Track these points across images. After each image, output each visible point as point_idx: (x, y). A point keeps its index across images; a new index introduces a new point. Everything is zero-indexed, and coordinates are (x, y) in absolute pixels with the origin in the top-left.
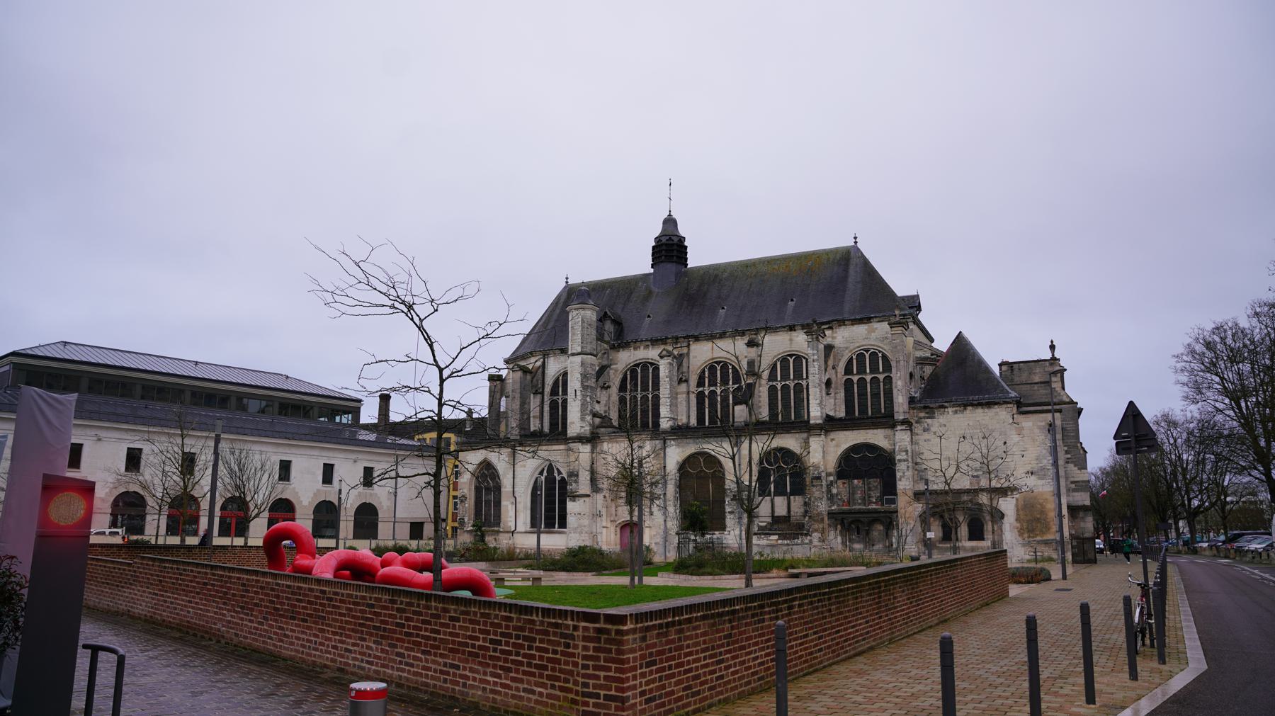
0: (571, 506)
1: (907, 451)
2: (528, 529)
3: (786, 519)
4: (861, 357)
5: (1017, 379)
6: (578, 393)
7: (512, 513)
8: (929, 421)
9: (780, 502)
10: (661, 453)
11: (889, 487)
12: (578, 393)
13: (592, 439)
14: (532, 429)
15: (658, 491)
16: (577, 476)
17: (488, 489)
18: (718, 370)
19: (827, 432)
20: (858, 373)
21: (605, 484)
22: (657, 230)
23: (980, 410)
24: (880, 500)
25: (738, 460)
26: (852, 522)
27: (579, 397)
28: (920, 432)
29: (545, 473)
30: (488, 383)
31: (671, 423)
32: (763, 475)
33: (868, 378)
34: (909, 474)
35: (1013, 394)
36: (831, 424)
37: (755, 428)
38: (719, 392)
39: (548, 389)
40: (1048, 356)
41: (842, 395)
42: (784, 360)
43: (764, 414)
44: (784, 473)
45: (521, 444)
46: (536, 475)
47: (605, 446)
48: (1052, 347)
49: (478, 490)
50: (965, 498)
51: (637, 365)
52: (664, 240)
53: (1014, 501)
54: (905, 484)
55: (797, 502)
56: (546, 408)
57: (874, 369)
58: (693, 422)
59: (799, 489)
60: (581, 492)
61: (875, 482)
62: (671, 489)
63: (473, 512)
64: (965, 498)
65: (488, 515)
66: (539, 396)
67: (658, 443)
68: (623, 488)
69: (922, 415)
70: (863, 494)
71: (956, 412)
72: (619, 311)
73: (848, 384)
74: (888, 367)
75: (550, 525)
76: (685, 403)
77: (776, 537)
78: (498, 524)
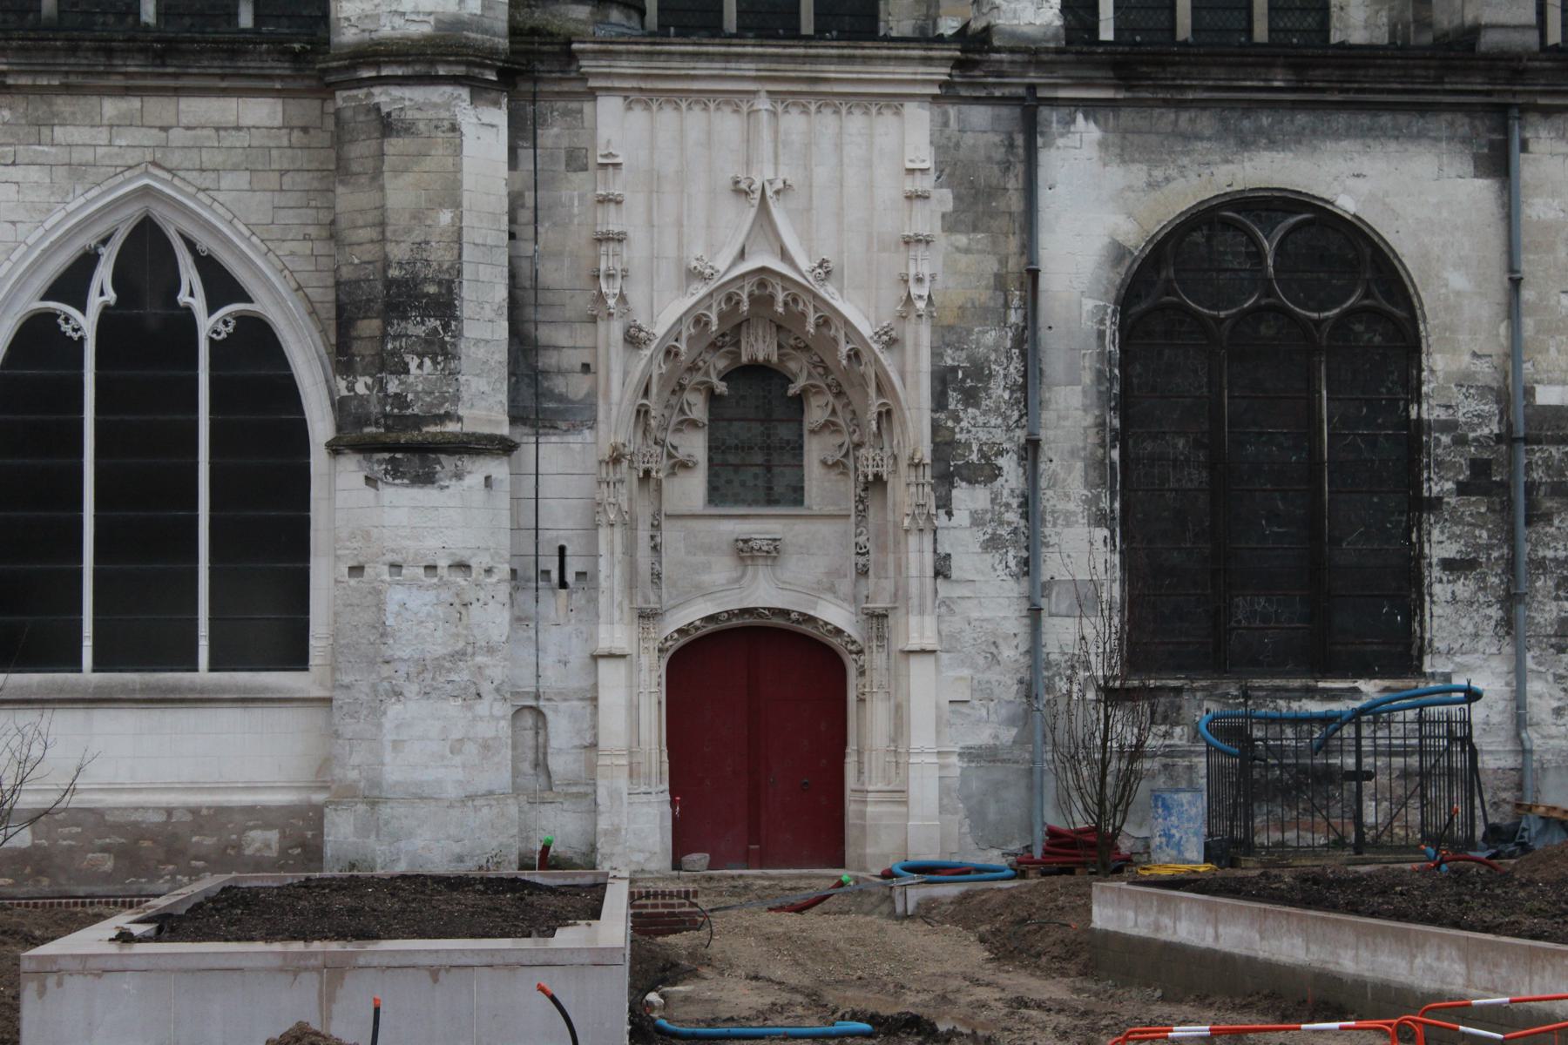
15: (980, 428)
16: (445, 306)
29: (102, 291)
47: (615, 125)
62: (1072, 412)
67: (981, 125)
68: (699, 409)
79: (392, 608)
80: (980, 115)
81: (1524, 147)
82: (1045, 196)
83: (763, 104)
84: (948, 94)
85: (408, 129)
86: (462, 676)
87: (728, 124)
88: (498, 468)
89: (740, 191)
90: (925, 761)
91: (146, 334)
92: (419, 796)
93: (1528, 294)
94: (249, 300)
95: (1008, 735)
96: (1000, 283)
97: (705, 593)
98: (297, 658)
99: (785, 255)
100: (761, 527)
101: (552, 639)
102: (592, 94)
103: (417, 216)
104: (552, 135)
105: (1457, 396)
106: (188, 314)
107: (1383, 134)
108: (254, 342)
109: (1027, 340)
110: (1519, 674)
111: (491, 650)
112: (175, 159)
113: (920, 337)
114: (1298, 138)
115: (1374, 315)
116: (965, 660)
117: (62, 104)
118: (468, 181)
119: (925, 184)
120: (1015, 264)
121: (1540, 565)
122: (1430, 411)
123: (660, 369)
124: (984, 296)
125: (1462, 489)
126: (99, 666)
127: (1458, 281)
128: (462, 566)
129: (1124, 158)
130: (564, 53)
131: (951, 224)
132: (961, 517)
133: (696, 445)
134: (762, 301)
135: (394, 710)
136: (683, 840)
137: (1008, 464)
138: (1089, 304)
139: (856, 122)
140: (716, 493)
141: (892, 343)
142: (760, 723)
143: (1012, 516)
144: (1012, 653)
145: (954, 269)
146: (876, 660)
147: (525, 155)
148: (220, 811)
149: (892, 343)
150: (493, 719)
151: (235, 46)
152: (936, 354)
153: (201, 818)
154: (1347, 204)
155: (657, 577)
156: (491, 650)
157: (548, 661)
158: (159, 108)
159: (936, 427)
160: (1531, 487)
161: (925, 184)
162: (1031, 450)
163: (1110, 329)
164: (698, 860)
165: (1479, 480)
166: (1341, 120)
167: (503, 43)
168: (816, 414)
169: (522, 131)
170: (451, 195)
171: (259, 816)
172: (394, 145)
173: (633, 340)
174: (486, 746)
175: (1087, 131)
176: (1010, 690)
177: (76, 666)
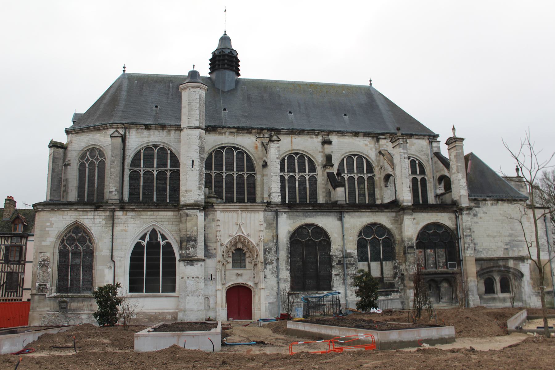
8: (477, 209)
10: (273, 225)
13: (206, 207)
15: (271, 257)
16: (195, 241)
17: (76, 254)
24: (446, 264)
25: (343, 232)
29: (147, 239)
30: (47, 152)
32: (361, 245)
37: (354, 207)
39: (128, 161)
40: (516, 175)
42: (350, 158)
47: (219, 215)
49: (63, 254)
50: (501, 263)
51: (223, 148)
53: (528, 266)
55: (388, 266)
59: (390, 256)
62: (283, 254)
64: (501, 263)
67: (270, 215)
68: (231, 255)
70: (436, 260)
71: (492, 204)
74: (423, 172)
75: (152, 288)
79: (187, 283)
80: (270, 213)
82: (279, 224)
83: (240, 212)
84: (265, 210)
85: (190, 216)
86: (197, 293)
87: (235, 215)
88: (202, 263)
89: (237, 224)
90: (263, 305)
91: (153, 245)
92: (191, 310)
93: (345, 237)
94: (167, 239)
95: (275, 300)
96: (273, 237)
97: (232, 281)
98: (174, 290)
99: (243, 233)
100: (240, 271)
101: (210, 288)
102: (216, 211)
103: (191, 228)
104: (210, 216)
105: (336, 251)
106: (159, 242)
107: (325, 215)
108: (169, 245)
109: (277, 244)
110: (346, 290)
112: (158, 220)
114: (314, 216)
115: (324, 240)
116: (269, 289)
117: (143, 213)
119: (262, 223)
120: (275, 234)
121: (348, 274)
122: (332, 253)
123: (225, 249)
125: (337, 264)
126: (146, 292)
127: (336, 235)
128: (198, 277)
129: (290, 219)
130: (212, 205)
131: (266, 228)
132: (268, 269)
133: (230, 260)
134: (240, 239)
135: (188, 298)
136: (229, 316)
137: (274, 262)
138: (285, 239)
139: (253, 214)
140: (233, 267)
142: (240, 299)
143: (275, 269)
144: (275, 289)
145: (267, 235)
146: (256, 290)
147: (207, 219)
148: (163, 313)
149: (258, 245)
151: (167, 205)
152: (264, 247)
153: (160, 314)
154: (320, 225)
155: (225, 279)
157: (209, 291)
158: (156, 213)
159: (264, 257)
160: (346, 264)
161: (262, 223)
162: (277, 260)
163: (288, 243)
164: (231, 319)
165: (339, 263)
166: (319, 213)
167: (204, 204)
168: (247, 255)
169: (206, 216)
170: (196, 225)
171: (168, 313)
172: (188, 218)
173: (222, 245)
174: (201, 303)
175: (285, 215)
176: (275, 294)
177: (142, 292)
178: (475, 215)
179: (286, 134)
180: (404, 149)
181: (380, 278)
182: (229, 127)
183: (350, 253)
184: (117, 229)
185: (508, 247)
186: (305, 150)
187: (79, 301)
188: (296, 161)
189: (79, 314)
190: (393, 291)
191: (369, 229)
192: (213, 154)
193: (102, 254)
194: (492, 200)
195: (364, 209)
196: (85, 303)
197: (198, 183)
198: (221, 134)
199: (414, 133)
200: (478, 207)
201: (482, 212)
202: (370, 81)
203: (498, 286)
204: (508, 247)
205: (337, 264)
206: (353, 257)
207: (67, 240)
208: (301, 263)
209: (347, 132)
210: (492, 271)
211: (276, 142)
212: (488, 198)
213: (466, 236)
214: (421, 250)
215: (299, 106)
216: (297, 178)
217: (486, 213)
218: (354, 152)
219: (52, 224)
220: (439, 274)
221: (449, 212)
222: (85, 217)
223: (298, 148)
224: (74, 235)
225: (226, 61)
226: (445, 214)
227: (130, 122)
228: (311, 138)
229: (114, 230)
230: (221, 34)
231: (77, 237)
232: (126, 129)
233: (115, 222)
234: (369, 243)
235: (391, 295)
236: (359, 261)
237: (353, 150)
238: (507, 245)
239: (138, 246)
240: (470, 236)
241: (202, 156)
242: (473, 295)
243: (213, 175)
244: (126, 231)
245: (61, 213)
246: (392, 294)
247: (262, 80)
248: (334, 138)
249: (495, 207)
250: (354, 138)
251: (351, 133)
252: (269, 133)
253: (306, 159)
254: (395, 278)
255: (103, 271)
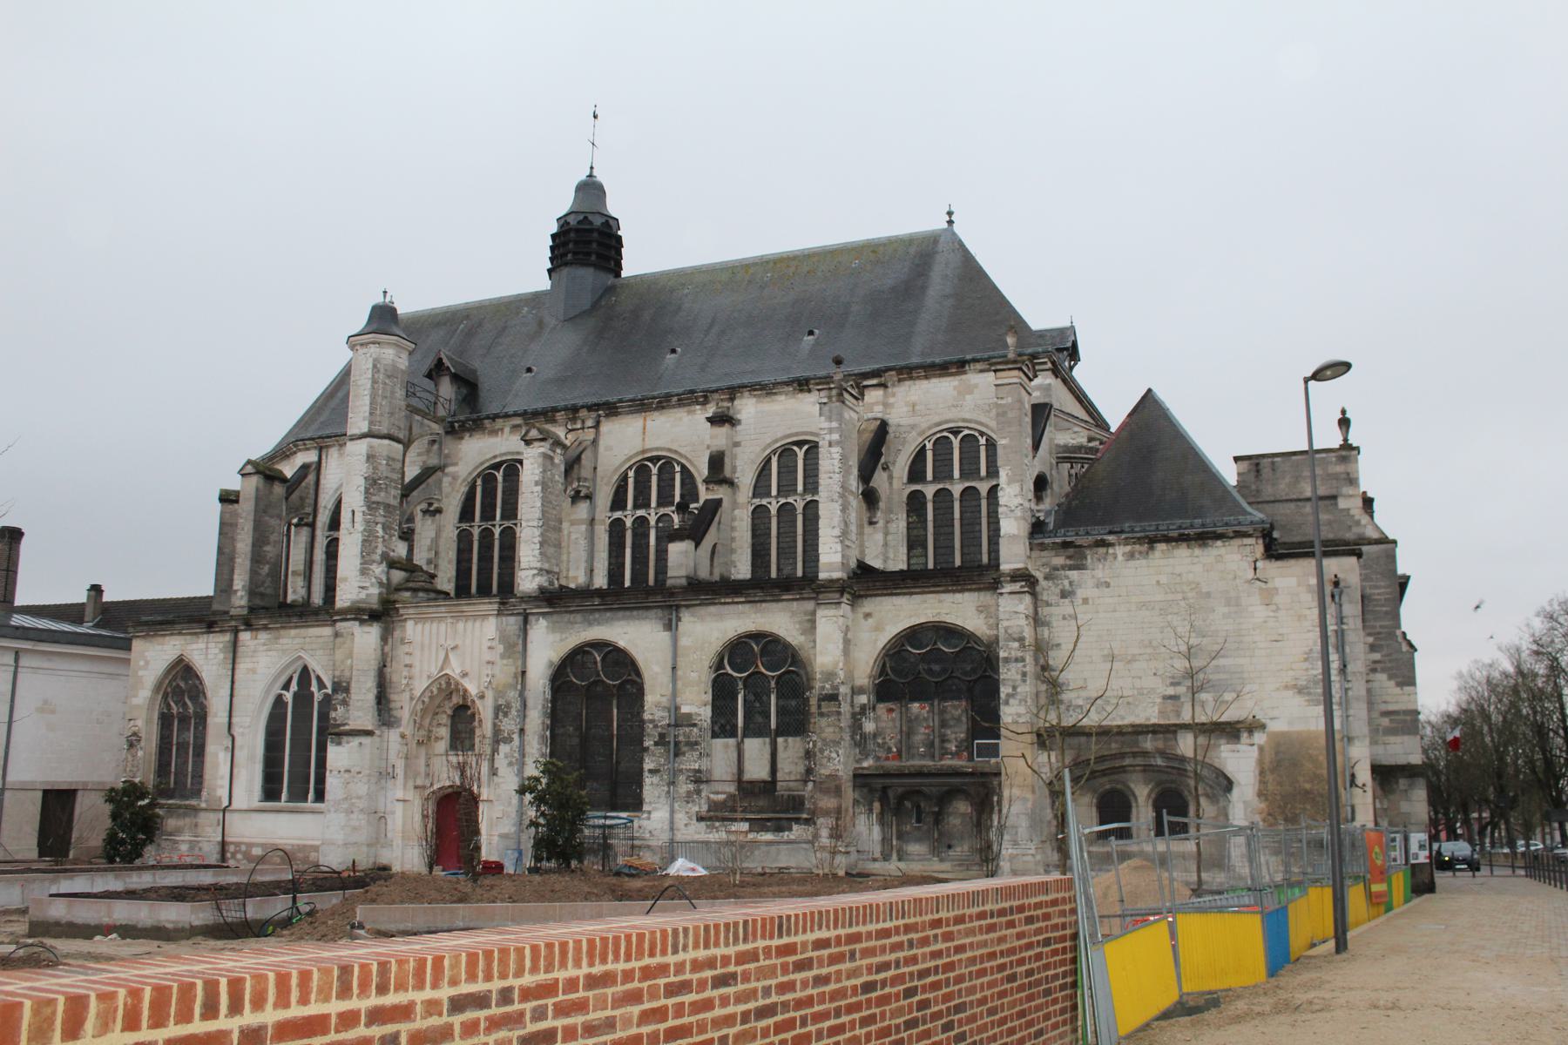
0: (338, 756)
1: (1021, 640)
2: (256, 804)
3: (769, 786)
4: (942, 445)
5: (1268, 491)
6: (359, 517)
7: (225, 770)
8: (1074, 574)
9: (755, 748)
10: (517, 647)
11: (986, 722)
12: (359, 517)
13: (383, 613)
14: (290, 598)
15: (509, 725)
16: (347, 690)
18: (653, 474)
19: (856, 598)
20: (936, 479)
21: (404, 706)
22: (564, 202)
23: (1183, 553)
24: (966, 747)
25: (676, 660)
26: (901, 798)
27: (360, 526)
28: (1053, 599)
29: (294, 687)
31: (542, 581)
32: (722, 691)
33: (957, 489)
34: (1026, 689)
35: (1259, 516)
36: (865, 581)
38: (652, 520)
39: (323, 518)
41: (900, 524)
42: (786, 453)
43: (742, 569)
44: (761, 685)
45: (249, 626)
46: (277, 690)
48: (1344, 423)
49: (165, 720)
50: (1148, 743)
51: (497, 466)
52: (572, 220)
53: (1254, 752)
54: (1014, 712)
55: (791, 750)
56: (320, 555)
57: (970, 471)
58: (600, 581)
59: (795, 723)
60: (353, 725)
61: (957, 709)
62: (536, 719)
63: (153, 766)
64: (1148, 743)
65: (181, 772)
66: (305, 531)
67: (512, 623)
68: (444, 719)
69: (1059, 561)
70: (927, 733)
71: (1131, 556)
72: (476, 364)
73: (915, 503)
75: (299, 795)
76: (583, 543)
77: (745, 826)
78: (197, 793)
80: (512, 619)
81: (679, 619)
82: (529, 646)
84: (500, 613)
88: (366, 740)
93: (680, 673)
104: (397, 634)
105: (655, 710)
107: (633, 618)
109: (522, 694)
110: (672, 812)
111: (359, 798)
113: (490, 695)
115: (633, 682)
118: (355, 651)
122: (646, 716)
124: (510, 680)
125: (656, 744)
127: (657, 669)
131: (503, 657)
132: (502, 754)
133: (444, 732)
137: (516, 737)
141: (482, 697)
145: (504, 671)
150: (359, 819)
154: (622, 644)
156: (359, 798)
158: (303, 631)
159: (495, 725)
160: (677, 744)
162: (522, 731)
163: (548, 690)
165: (662, 741)
166: (621, 614)
170: (350, 656)
174: (355, 829)
175: (543, 622)
176: (514, 815)
178: (1064, 595)
179: (631, 412)
180: (830, 419)
181: (764, 782)
182: (507, 416)
183: (689, 715)
184: (242, 667)
185: (1181, 690)
186: (674, 447)
187: (179, 816)
188: (654, 479)
189: (176, 842)
190: (797, 821)
191: (738, 650)
192: (479, 482)
193: (217, 720)
194: (1126, 542)
195: (727, 595)
196: (188, 820)
197: (358, 561)
198: (494, 432)
199: (968, 357)
200: (1080, 567)
201: (1090, 583)
202: (950, 213)
203: (1143, 815)
204: (1181, 690)
205: (656, 744)
206: (695, 725)
207: (174, 692)
208: (576, 741)
209: (776, 384)
210: (1123, 769)
211: (536, 444)
212: (1111, 538)
213: (1007, 660)
214: (891, 705)
215: (707, 332)
216: (653, 523)
217: (1108, 585)
218: (797, 434)
219: (147, 663)
220: (930, 775)
221: (979, 590)
222: (195, 646)
223: (658, 444)
224: (182, 685)
225: (594, 245)
226: (967, 594)
227: (328, 432)
228: (689, 412)
229: (237, 672)
230: (583, 177)
231: (182, 684)
232: (321, 449)
233: (239, 654)
234: (741, 685)
235: (790, 829)
236: (715, 735)
237: (794, 430)
238: (1172, 684)
239: (279, 702)
240: (1017, 660)
241: (374, 498)
242: (1015, 843)
243: (497, 531)
244: (254, 671)
245: (160, 639)
246: (795, 827)
247: (694, 268)
248: (747, 408)
249: (1141, 562)
250: (800, 396)
251: (787, 384)
252: (594, 415)
253: (678, 469)
254: (805, 782)
255: (216, 755)
